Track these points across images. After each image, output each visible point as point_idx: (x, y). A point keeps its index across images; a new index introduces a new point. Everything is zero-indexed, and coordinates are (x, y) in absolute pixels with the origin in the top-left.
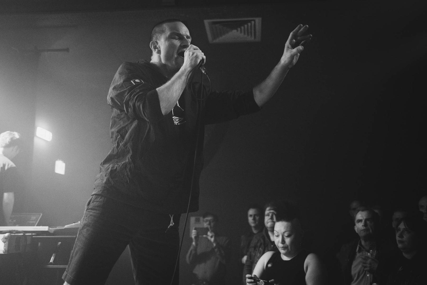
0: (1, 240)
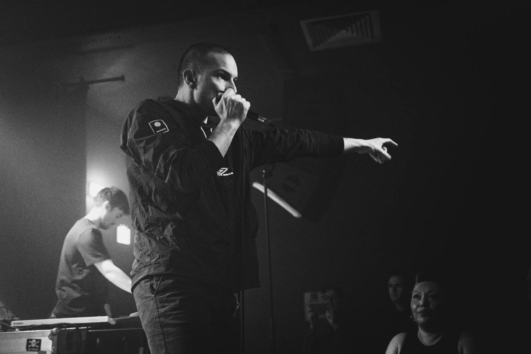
0: (47, 337)
